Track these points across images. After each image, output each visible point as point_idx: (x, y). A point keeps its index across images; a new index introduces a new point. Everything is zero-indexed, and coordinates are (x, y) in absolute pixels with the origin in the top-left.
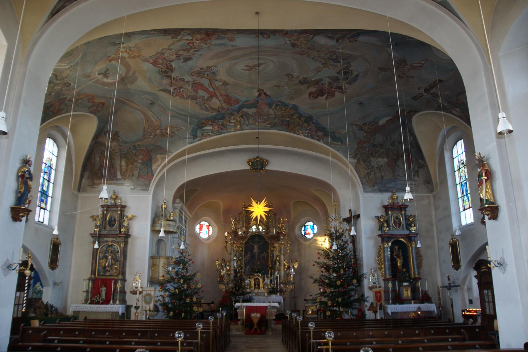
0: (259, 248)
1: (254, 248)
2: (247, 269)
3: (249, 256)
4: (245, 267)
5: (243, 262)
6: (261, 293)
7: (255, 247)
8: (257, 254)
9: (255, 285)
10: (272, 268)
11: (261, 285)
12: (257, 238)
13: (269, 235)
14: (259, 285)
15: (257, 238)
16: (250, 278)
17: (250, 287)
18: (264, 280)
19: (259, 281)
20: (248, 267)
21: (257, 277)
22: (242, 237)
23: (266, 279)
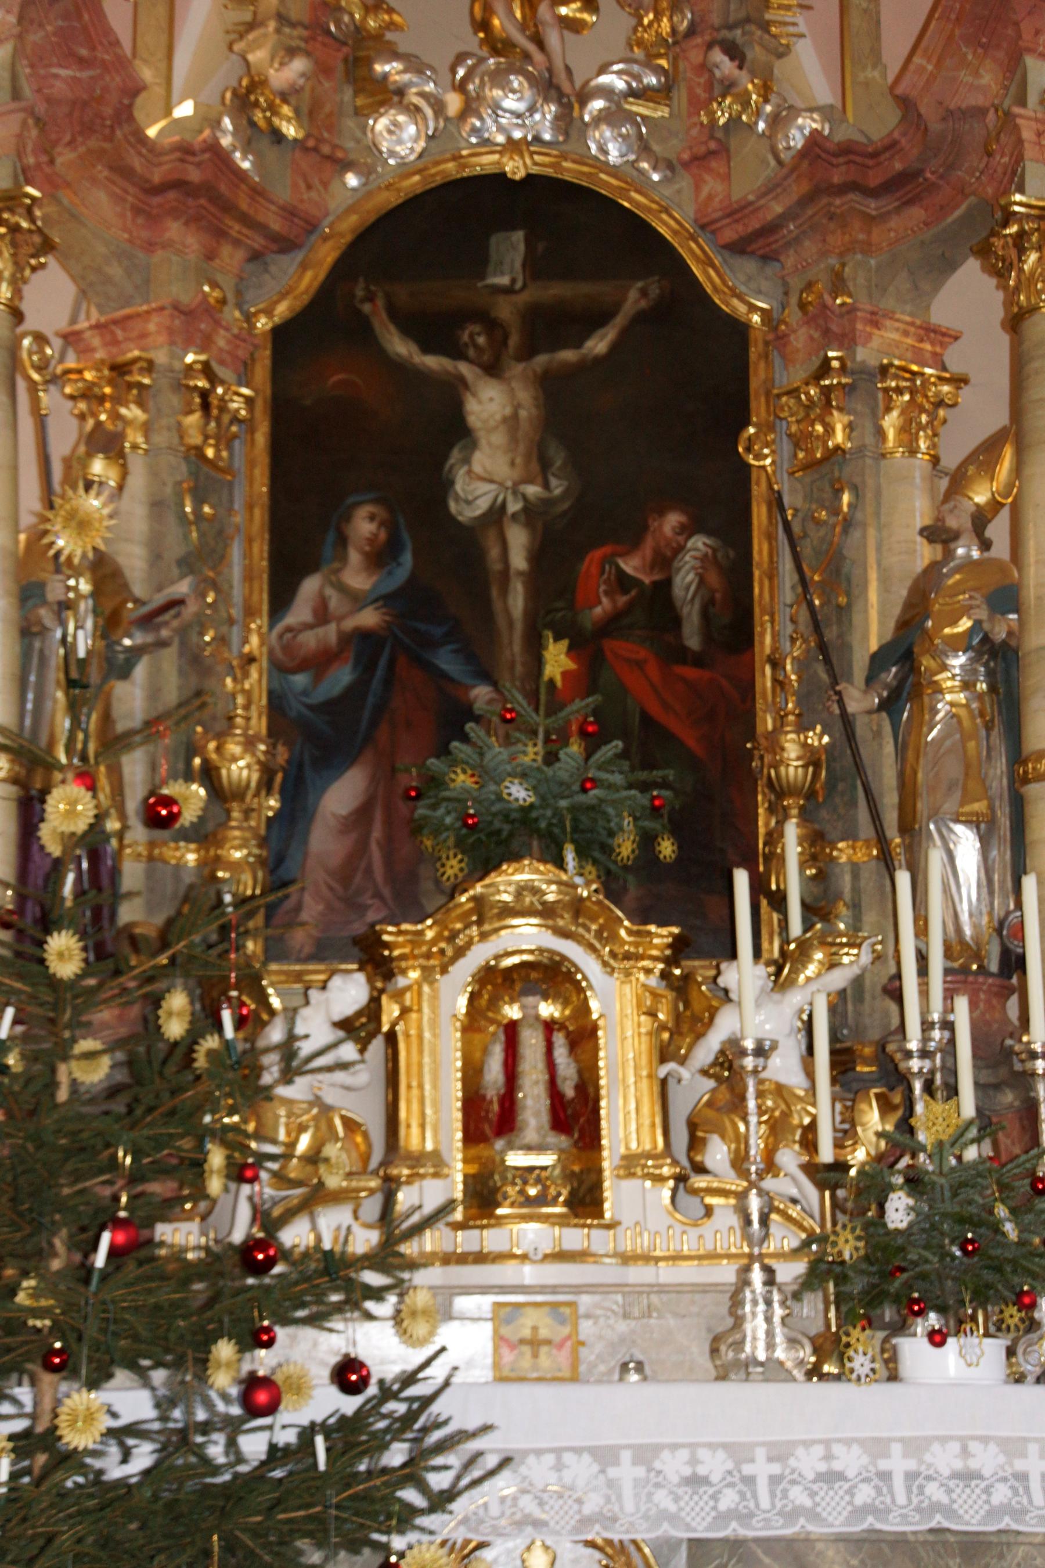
0: (563, 419)
1: (456, 431)
2: (324, 841)
3: (357, 577)
4: (294, 789)
5: (247, 693)
6: (639, 1302)
7: (489, 404)
8: (519, 545)
9: (488, 1118)
10: (837, 788)
11: (626, 1121)
12: (509, 256)
13: (747, 177)
14: (576, 1116)
15: (509, 256)
16: (379, 966)
17: (393, 1158)
18: (686, 1010)
19: (582, 1036)
20: (342, 795)
21: (525, 937)
22: (195, 191)
23: (745, 975)
